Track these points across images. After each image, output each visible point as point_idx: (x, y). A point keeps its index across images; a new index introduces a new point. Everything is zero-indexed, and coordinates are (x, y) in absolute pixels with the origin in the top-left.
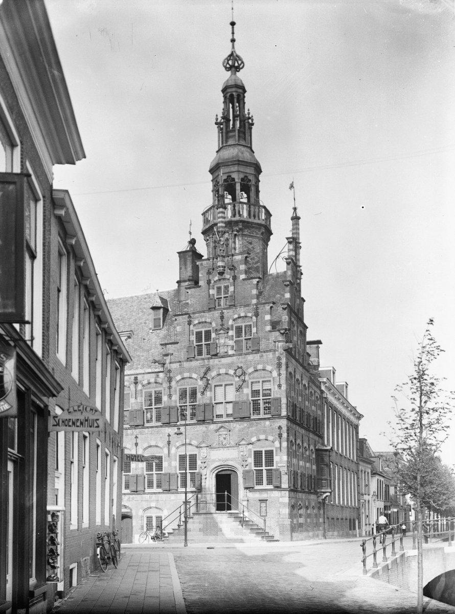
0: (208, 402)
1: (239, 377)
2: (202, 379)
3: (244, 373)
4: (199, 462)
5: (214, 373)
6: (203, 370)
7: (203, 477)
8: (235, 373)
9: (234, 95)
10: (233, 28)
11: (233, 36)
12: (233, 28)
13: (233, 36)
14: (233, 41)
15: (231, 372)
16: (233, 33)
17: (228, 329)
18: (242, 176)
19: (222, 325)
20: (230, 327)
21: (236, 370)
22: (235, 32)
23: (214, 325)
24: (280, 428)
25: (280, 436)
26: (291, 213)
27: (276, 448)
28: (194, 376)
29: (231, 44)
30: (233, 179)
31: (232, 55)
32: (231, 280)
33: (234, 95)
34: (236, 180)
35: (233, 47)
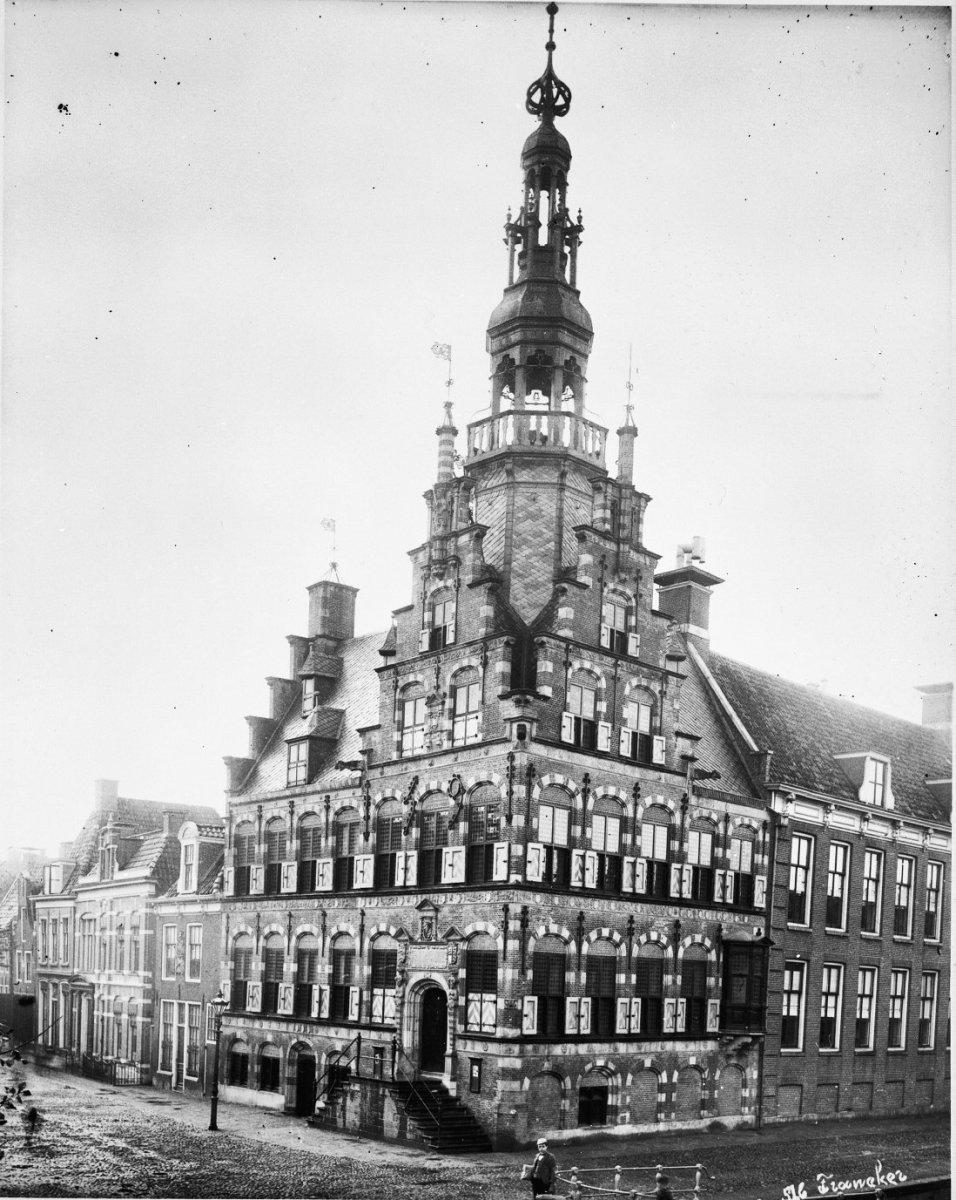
5: (421, 790)
6: (409, 782)
8: (450, 790)
9: (548, 162)
10: (552, 19)
11: (551, 37)
12: (552, 19)
13: (551, 37)
16: (551, 31)
18: (531, 350)
19: (438, 687)
21: (451, 783)
22: (555, 28)
29: (546, 53)
30: (513, 360)
31: (550, 74)
33: (548, 162)
34: (517, 363)
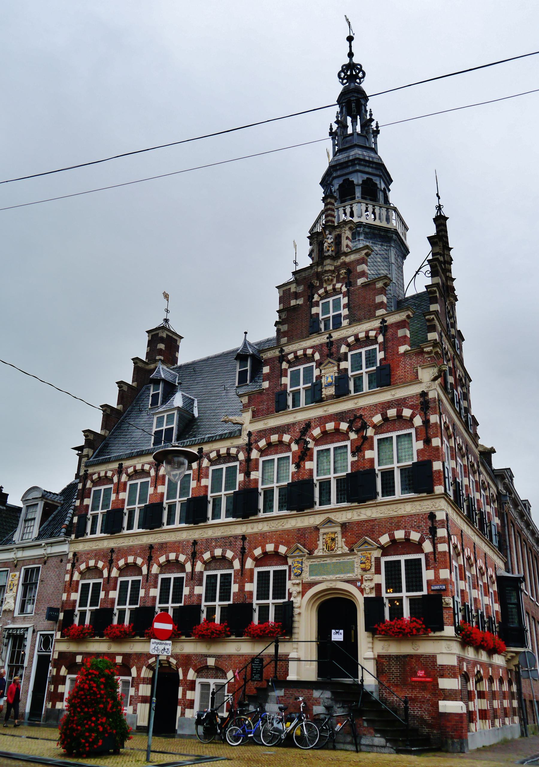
0: (306, 477)
1: (357, 432)
2: (297, 442)
3: (364, 427)
4: (289, 584)
7: (296, 611)
14: (350, 39)
15: (344, 426)
17: (339, 360)
20: (342, 357)
23: (317, 356)
24: (432, 516)
25: (433, 531)
26: (434, 213)
27: (427, 555)
28: (286, 438)
32: (344, 289)
35: (350, 47)
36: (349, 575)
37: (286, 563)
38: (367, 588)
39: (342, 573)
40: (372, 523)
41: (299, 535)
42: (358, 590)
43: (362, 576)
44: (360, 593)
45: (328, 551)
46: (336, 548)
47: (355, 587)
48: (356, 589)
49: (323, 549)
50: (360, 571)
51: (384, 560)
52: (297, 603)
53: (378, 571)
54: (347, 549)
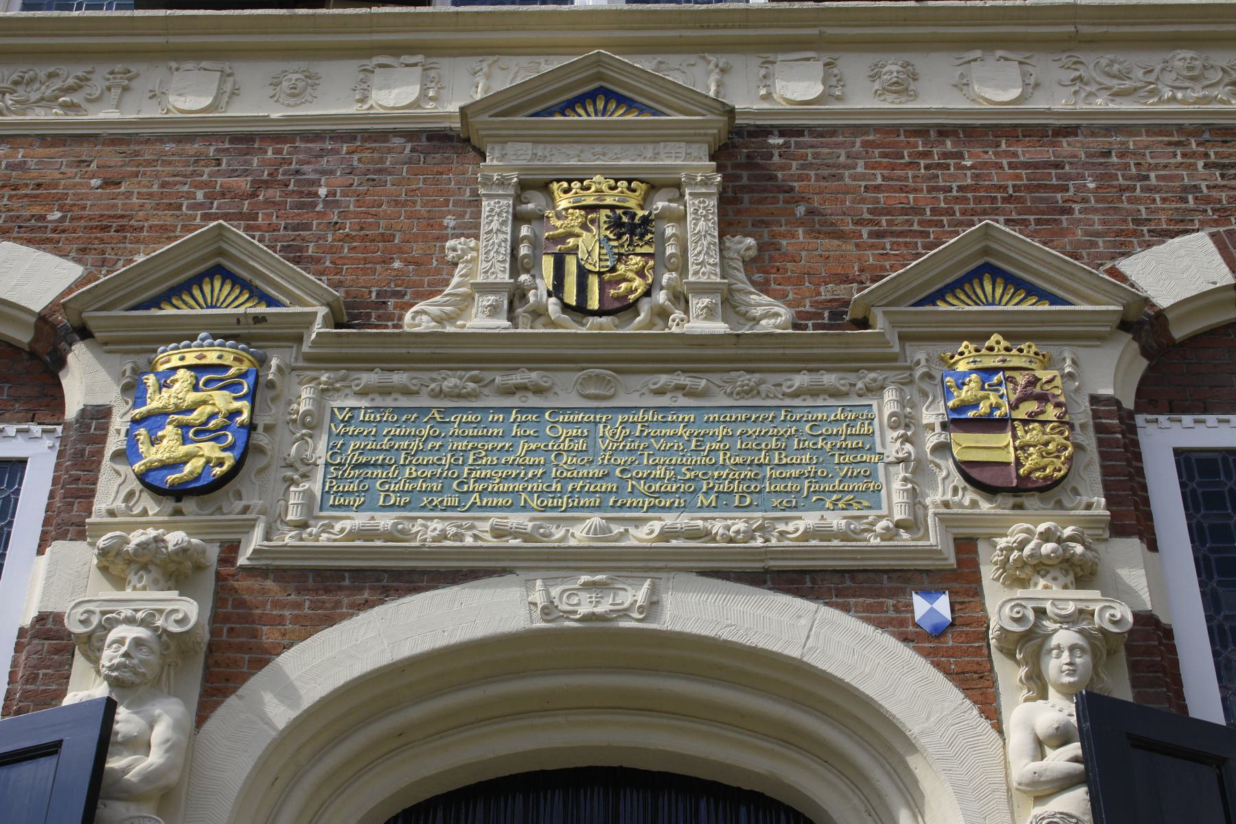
36: (809, 520)
37: (47, 401)
38: (1064, 637)
39: (723, 501)
40: (1025, 152)
41: (244, 184)
42: (923, 666)
43: (966, 546)
44: (952, 696)
45: (580, 310)
46: (661, 297)
47: (887, 641)
48: (905, 652)
49: (517, 296)
50: (945, 489)
51: (1164, 439)
52: (140, 744)
53: (1131, 516)
54: (785, 313)
